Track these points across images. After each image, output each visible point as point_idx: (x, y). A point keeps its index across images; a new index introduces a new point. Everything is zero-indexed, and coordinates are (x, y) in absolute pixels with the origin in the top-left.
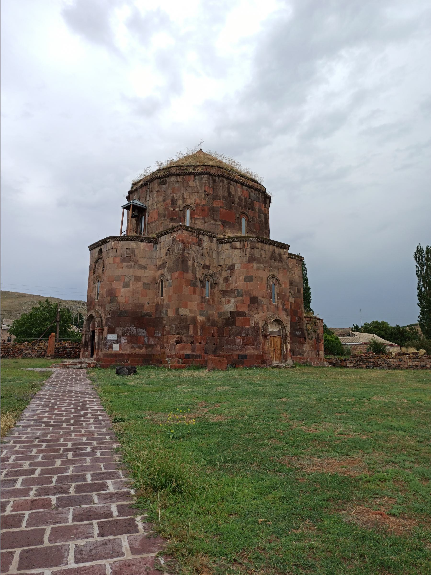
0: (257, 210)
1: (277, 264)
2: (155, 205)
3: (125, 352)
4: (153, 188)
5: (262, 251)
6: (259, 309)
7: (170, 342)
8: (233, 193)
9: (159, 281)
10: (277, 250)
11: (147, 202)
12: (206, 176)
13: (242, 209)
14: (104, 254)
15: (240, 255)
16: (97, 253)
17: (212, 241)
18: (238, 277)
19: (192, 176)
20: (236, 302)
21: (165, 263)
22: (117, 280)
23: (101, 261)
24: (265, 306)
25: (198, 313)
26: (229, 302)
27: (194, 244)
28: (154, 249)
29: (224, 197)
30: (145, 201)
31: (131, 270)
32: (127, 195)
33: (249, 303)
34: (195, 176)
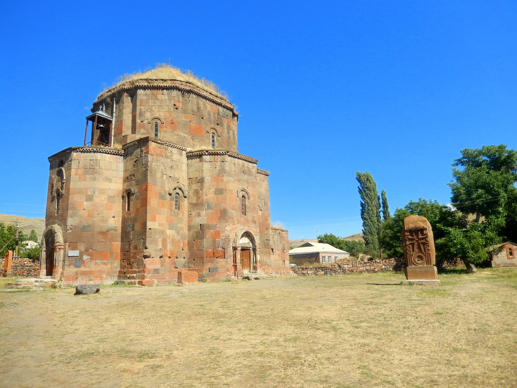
0: (226, 126)
1: (245, 177)
5: (231, 164)
6: (229, 222)
7: (138, 256)
8: (201, 108)
13: (211, 124)
15: (210, 168)
17: (181, 155)
18: (208, 189)
22: (79, 193)
24: (236, 218)
25: (167, 226)
26: (199, 215)
27: (163, 157)
29: (193, 111)
32: (92, 107)
33: (220, 215)
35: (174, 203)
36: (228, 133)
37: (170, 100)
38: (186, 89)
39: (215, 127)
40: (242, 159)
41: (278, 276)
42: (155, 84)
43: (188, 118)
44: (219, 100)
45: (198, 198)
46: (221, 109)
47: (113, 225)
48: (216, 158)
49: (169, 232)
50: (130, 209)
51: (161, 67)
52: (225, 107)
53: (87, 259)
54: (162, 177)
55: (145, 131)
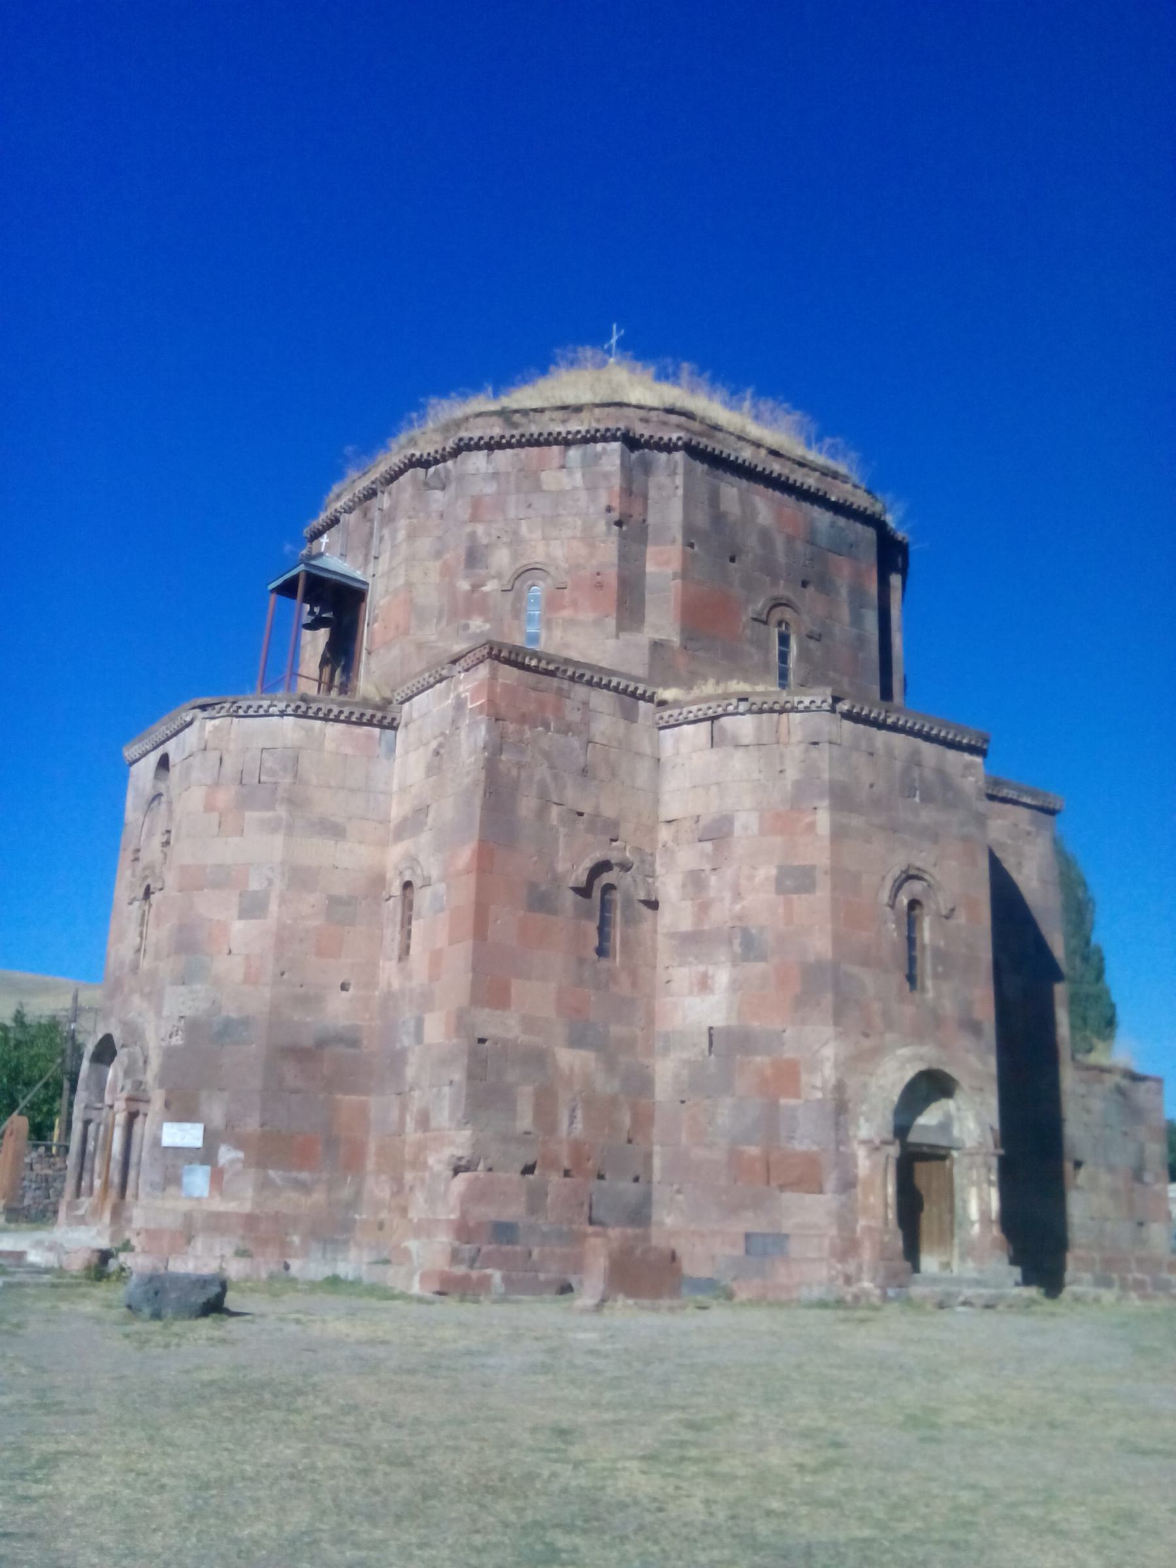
0: (844, 592)
1: (927, 816)
2: (402, 571)
3: (232, 1206)
4: (394, 507)
7: (431, 1160)
8: (731, 518)
9: (396, 889)
10: (927, 748)
11: (371, 565)
12: (616, 446)
13: (775, 583)
14: (175, 772)
15: (755, 776)
16: (151, 774)
17: (630, 716)
19: (556, 449)
20: (735, 986)
21: (421, 811)
22: (217, 885)
23: (163, 806)
24: (876, 1006)
26: (704, 984)
27: (547, 726)
28: (382, 750)
30: (366, 562)
31: (279, 840)
34: (566, 451)
35: (592, 927)
36: (857, 620)
37: (592, 489)
38: (661, 439)
39: (792, 597)
40: (910, 732)
41: (1108, 1296)
42: (534, 429)
43: (667, 563)
44: (811, 481)
45: (703, 908)
46: (822, 518)
47: (343, 1022)
48: (783, 729)
49: (568, 1058)
50: (411, 952)
51: (573, 363)
52: (840, 508)
53: (233, 1162)
54: (542, 813)
55: (488, 626)
